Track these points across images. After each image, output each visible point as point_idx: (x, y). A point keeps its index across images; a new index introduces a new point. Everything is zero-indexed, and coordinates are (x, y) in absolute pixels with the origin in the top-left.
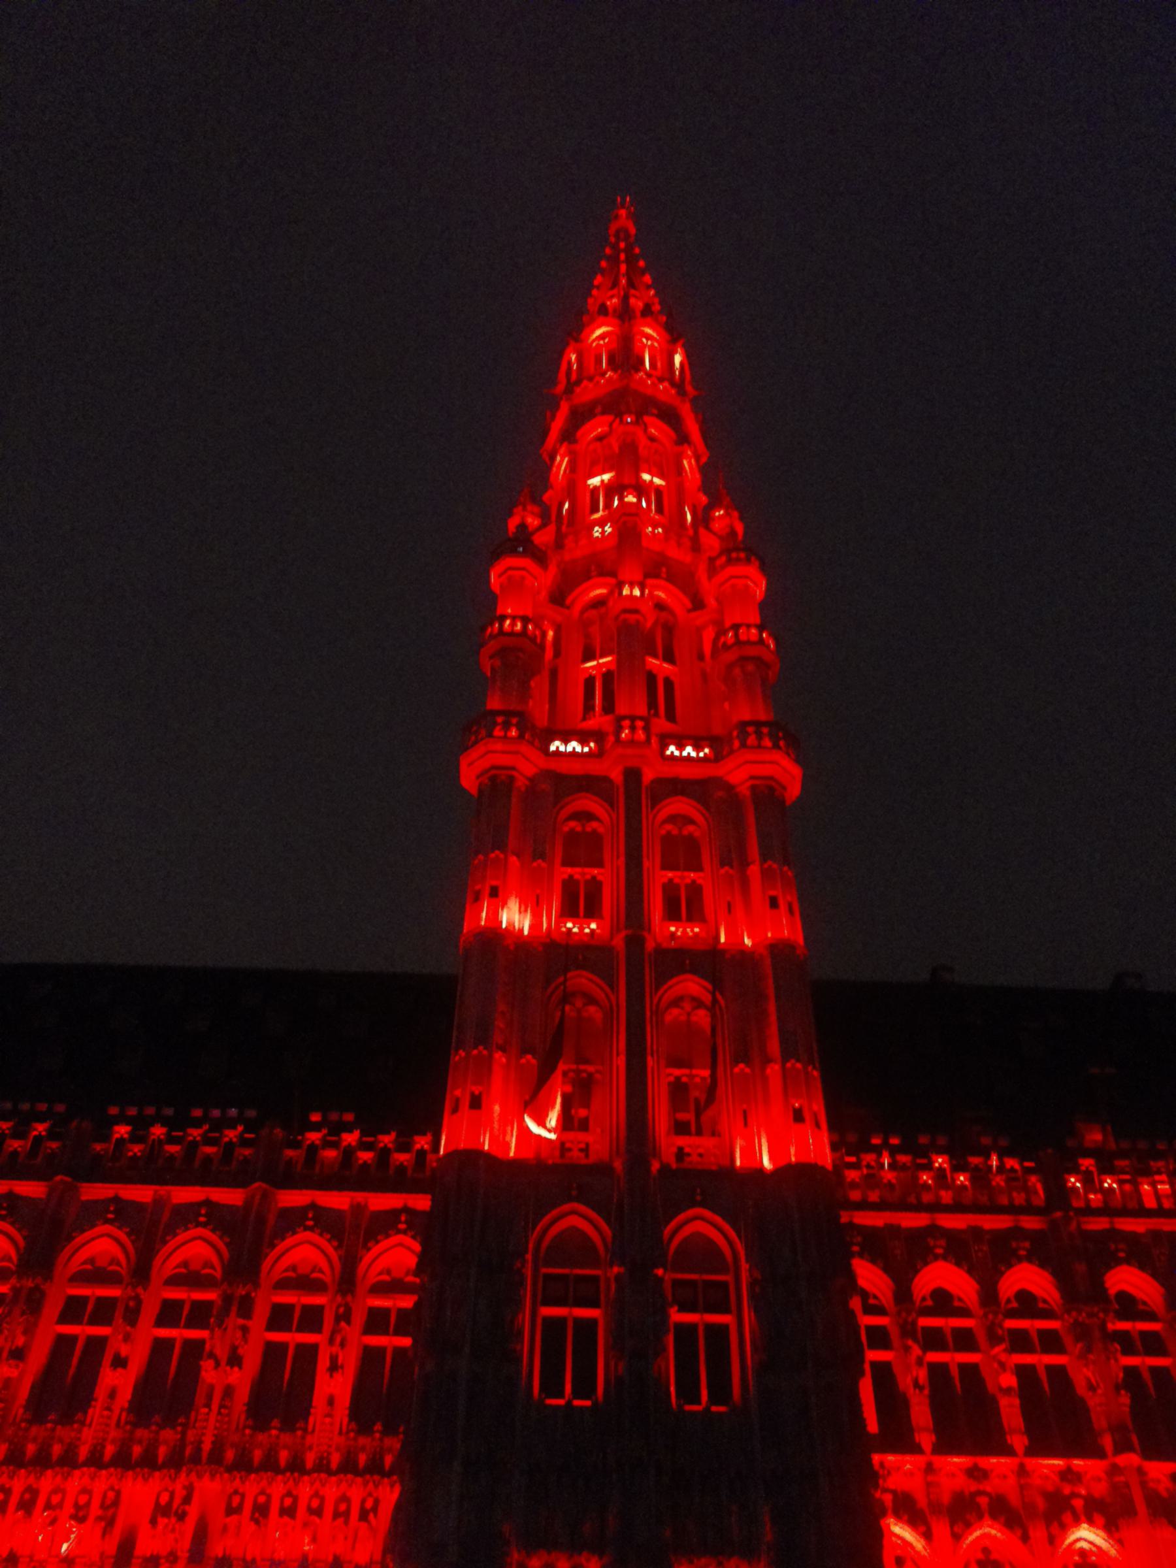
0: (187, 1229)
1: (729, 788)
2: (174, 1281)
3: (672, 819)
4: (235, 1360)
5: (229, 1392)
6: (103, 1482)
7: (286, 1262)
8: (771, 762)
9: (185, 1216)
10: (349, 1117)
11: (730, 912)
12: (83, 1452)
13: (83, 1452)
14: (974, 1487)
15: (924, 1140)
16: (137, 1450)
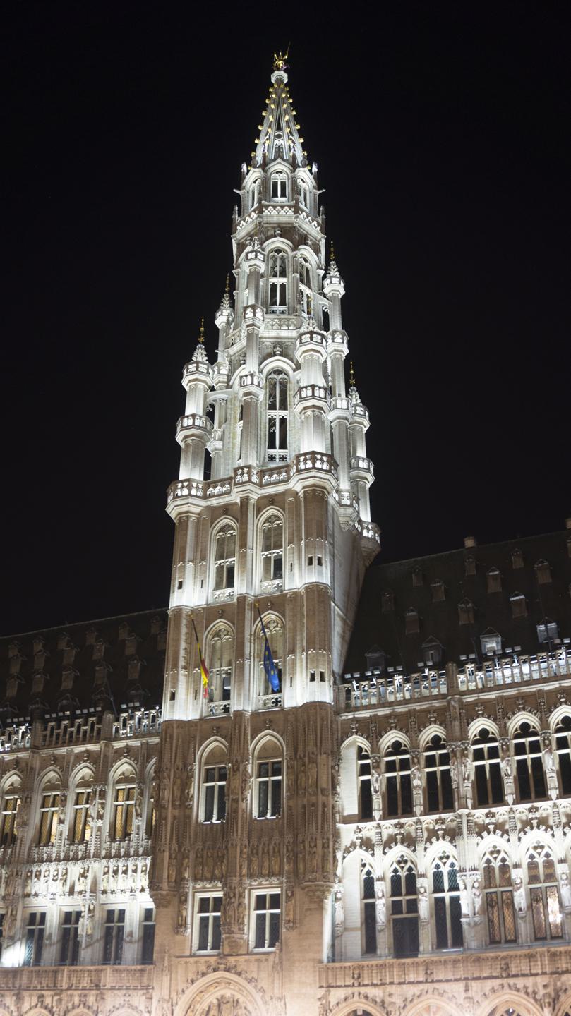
0: (80, 764)
1: (297, 493)
2: (78, 786)
3: (267, 521)
4: (100, 817)
5: (99, 829)
6: (61, 866)
7: (119, 771)
8: (311, 477)
9: (79, 758)
10: (137, 704)
11: (291, 571)
12: (54, 856)
13: (54, 856)
14: (396, 831)
15: (391, 670)
16: (71, 854)
